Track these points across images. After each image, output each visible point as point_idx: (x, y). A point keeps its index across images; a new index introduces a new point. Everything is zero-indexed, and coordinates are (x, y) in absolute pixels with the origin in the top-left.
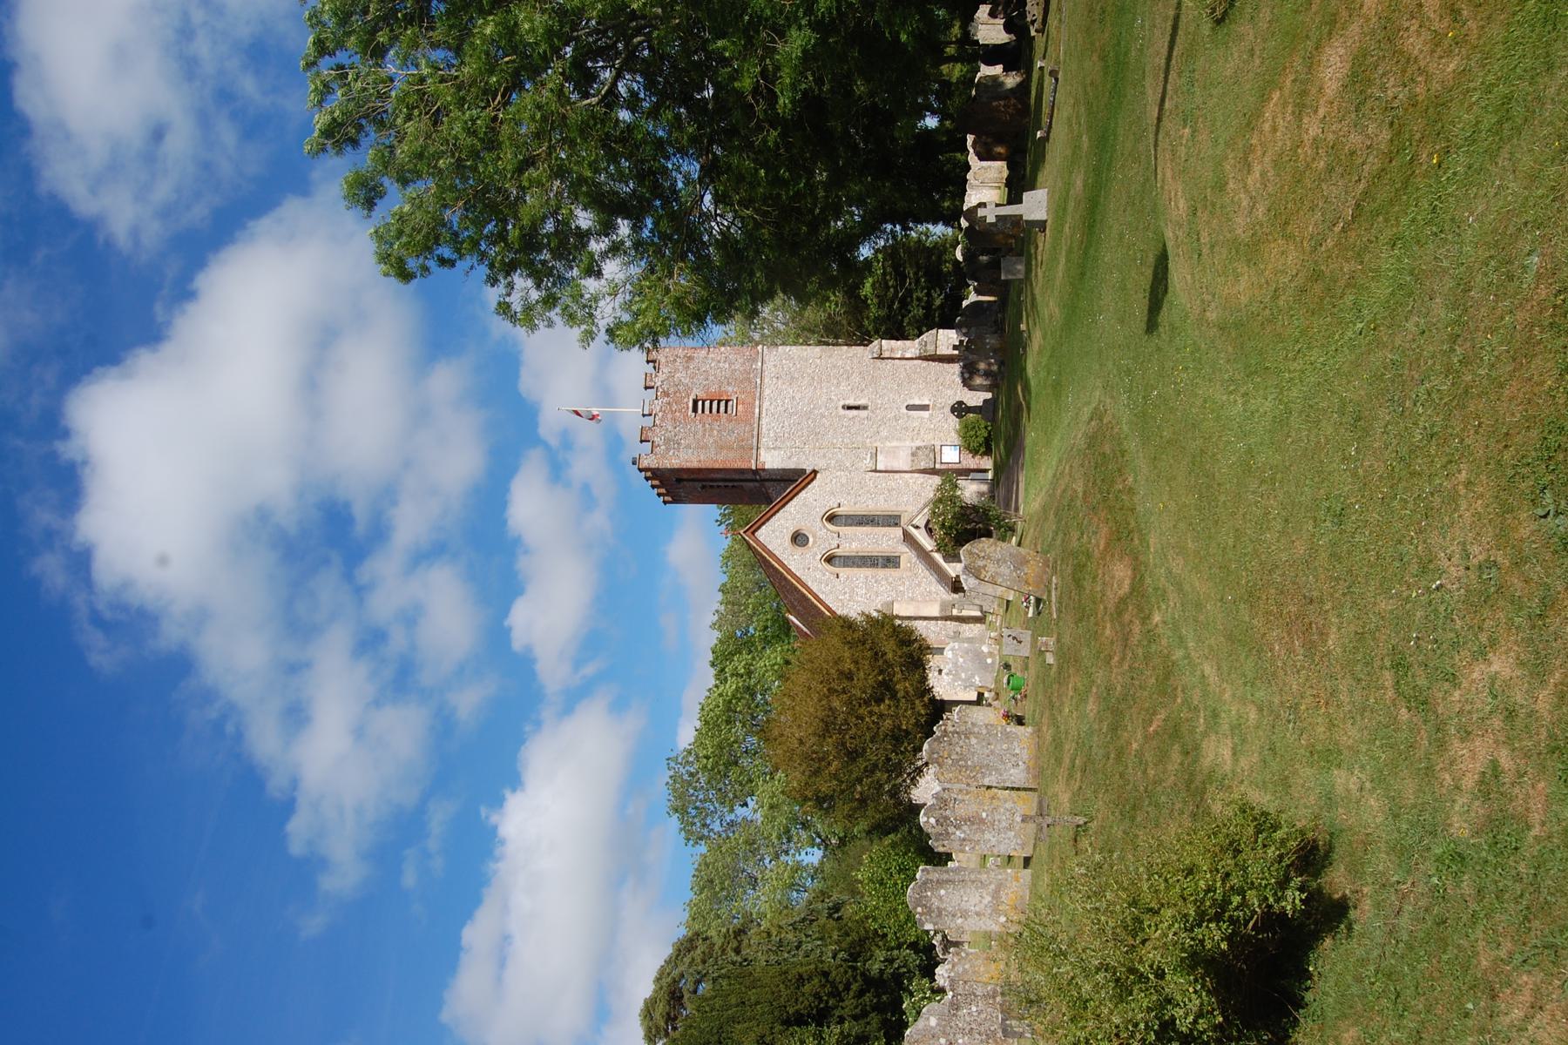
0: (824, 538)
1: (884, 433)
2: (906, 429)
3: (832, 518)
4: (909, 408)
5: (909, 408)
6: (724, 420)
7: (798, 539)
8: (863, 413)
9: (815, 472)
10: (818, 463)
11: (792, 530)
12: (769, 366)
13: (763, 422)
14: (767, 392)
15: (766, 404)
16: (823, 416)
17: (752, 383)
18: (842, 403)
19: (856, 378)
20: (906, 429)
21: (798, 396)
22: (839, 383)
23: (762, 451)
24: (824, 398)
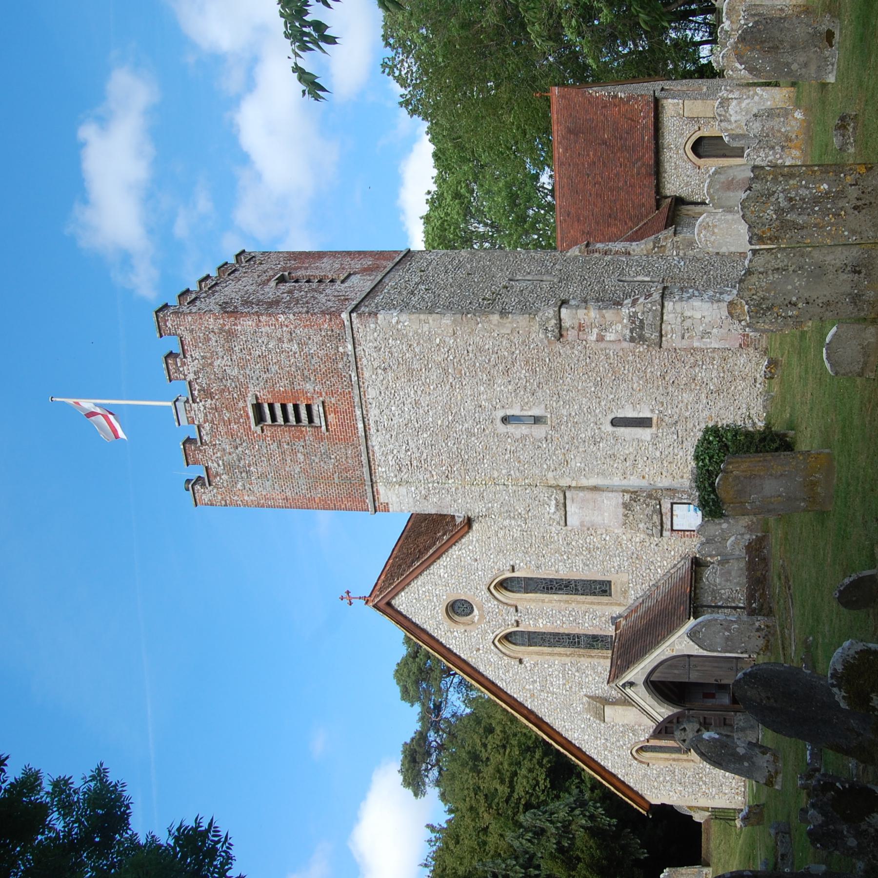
0: (495, 614)
1: (576, 464)
2: (613, 456)
3: (505, 585)
4: (616, 422)
5: (616, 422)
6: (309, 438)
7: (458, 609)
8: (539, 431)
9: (469, 522)
10: (476, 509)
11: (446, 599)
12: (366, 348)
13: (374, 441)
14: (371, 393)
15: (373, 414)
16: (470, 433)
17: (343, 373)
18: (501, 414)
19: (521, 372)
20: (613, 456)
21: (424, 401)
22: (491, 381)
23: (381, 488)
24: (470, 405)
